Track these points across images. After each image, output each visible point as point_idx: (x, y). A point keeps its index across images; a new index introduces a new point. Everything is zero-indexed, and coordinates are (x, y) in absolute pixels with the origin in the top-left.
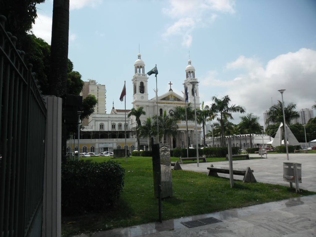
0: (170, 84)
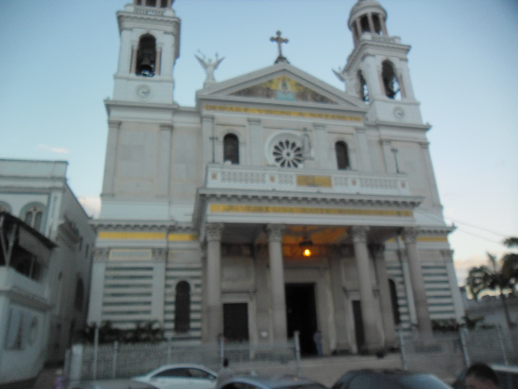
0: (279, 39)
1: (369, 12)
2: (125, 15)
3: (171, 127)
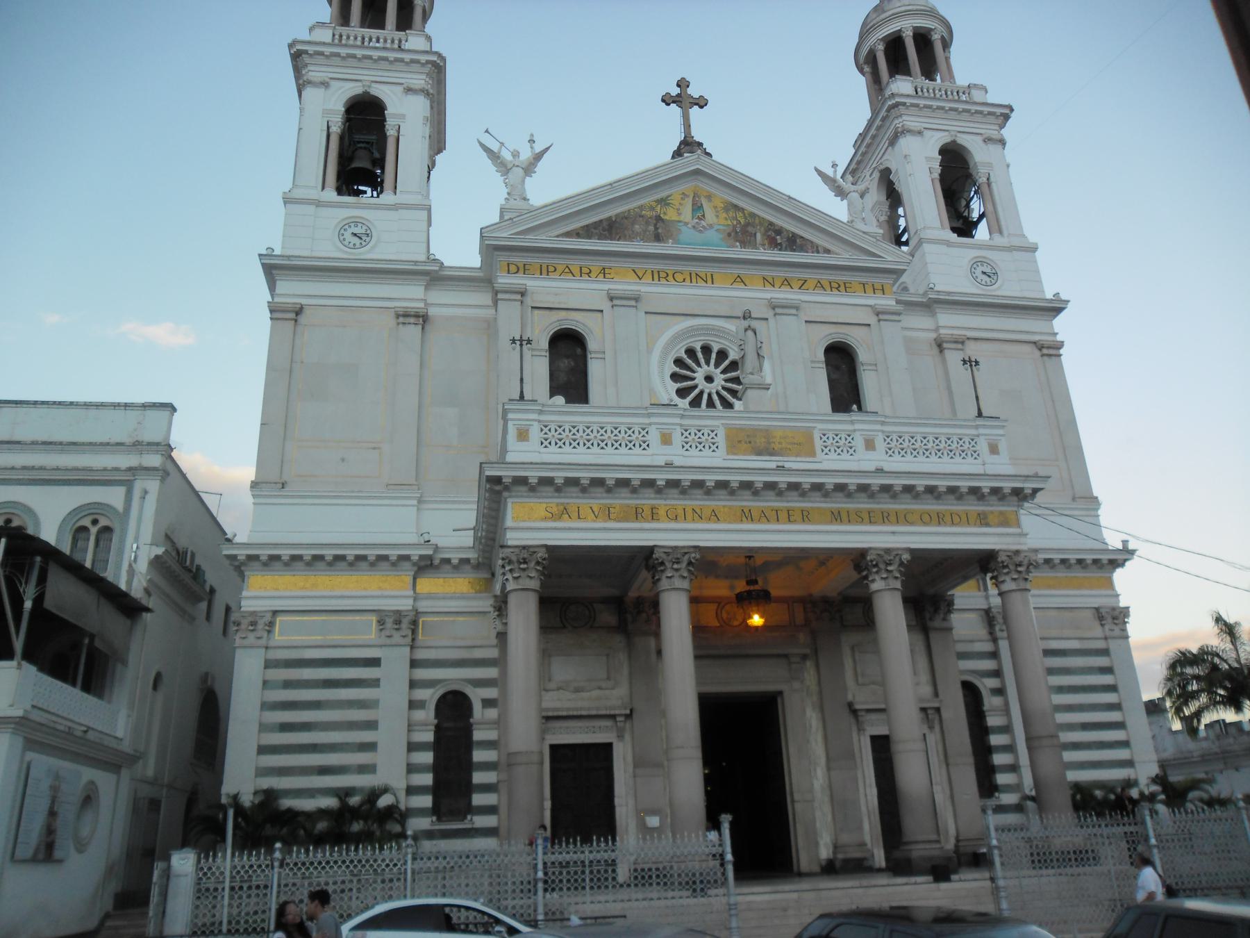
1: (907, 26)
2: (311, 49)
3: (422, 318)
